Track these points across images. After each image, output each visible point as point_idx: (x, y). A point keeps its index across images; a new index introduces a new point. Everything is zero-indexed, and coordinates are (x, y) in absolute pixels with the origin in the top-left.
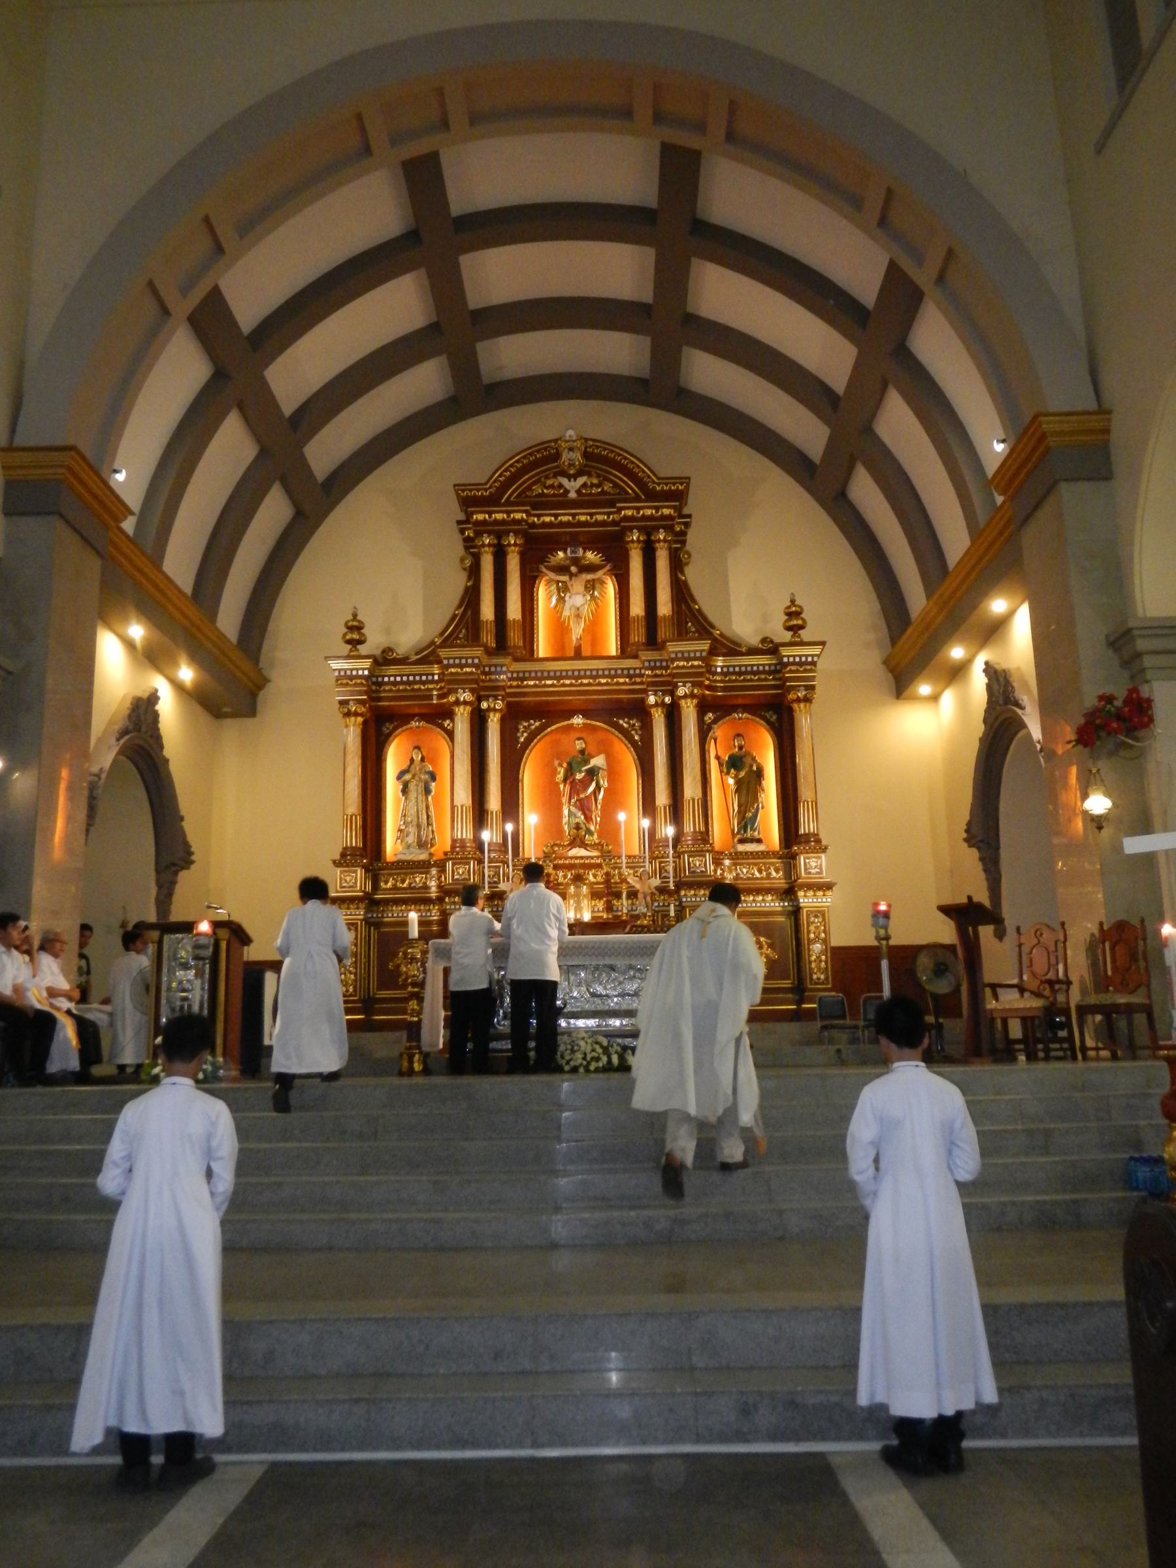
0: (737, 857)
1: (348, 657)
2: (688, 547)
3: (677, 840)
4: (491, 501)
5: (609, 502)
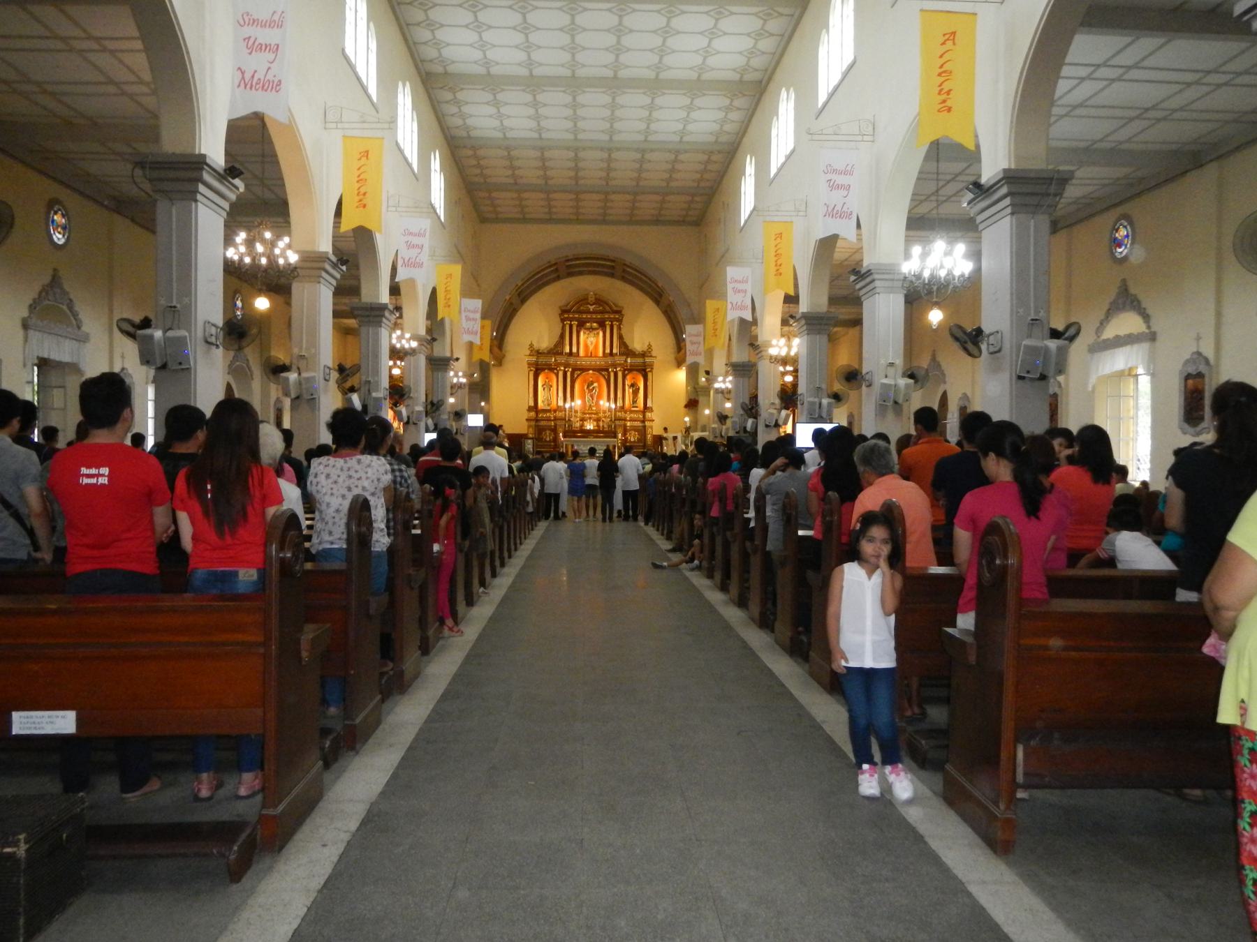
0: (632, 412)
3: (615, 409)
5: (601, 312)
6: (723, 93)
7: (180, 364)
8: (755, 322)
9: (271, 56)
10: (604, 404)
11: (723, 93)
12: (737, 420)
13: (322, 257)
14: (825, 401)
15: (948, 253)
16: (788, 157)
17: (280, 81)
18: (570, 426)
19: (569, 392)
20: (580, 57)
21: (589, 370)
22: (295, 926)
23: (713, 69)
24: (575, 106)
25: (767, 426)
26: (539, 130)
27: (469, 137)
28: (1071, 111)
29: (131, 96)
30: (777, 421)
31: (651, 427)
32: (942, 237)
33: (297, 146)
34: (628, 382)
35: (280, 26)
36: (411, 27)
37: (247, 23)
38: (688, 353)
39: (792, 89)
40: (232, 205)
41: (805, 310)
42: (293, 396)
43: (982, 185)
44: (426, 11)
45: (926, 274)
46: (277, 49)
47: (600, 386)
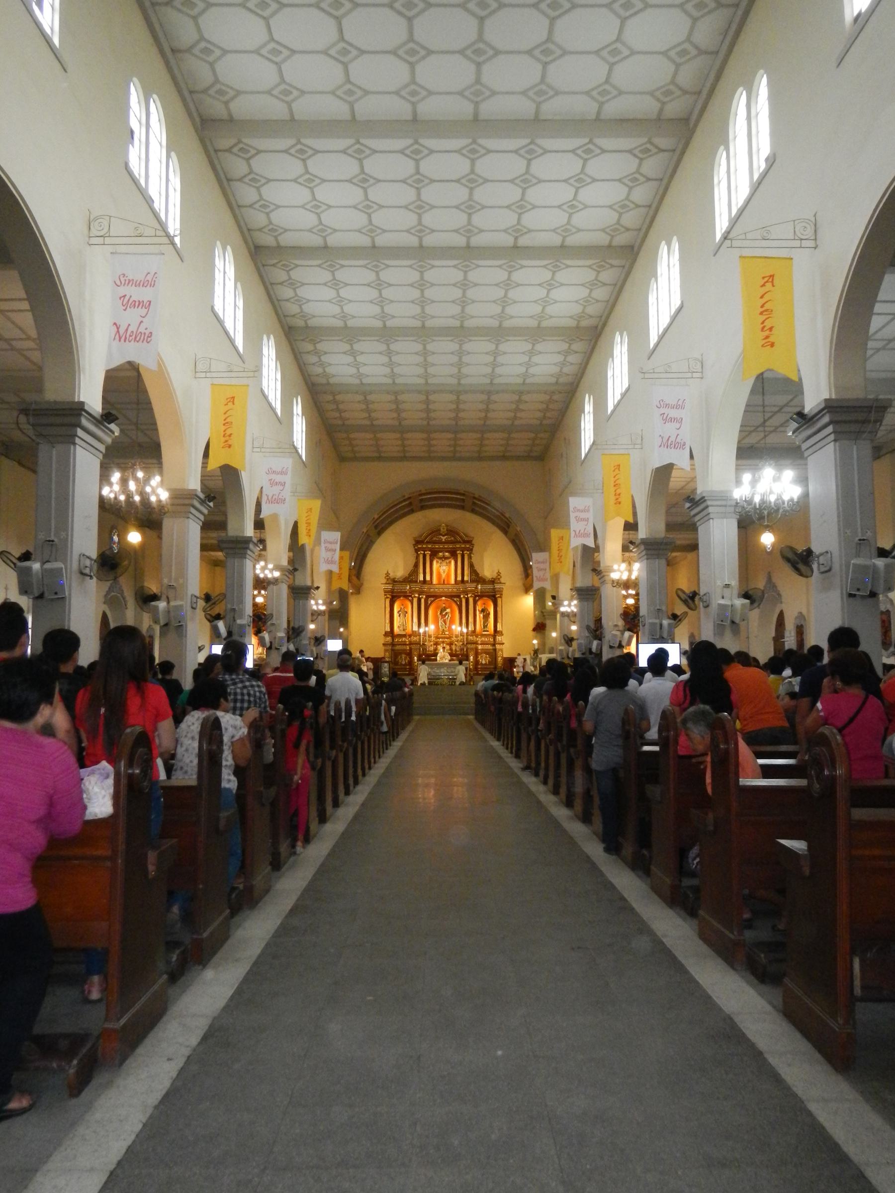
0: (483, 635)
1: (386, 584)
2: (474, 552)
3: (467, 633)
4: (422, 542)
6: (562, 338)
7: (56, 593)
8: (597, 549)
9: (144, 311)
10: (456, 628)
11: (562, 338)
12: (583, 642)
13: (192, 495)
14: (665, 622)
15: (776, 479)
16: (623, 395)
17: (151, 333)
18: (425, 649)
19: (422, 617)
20: (429, 310)
21: (442, 596)
22: (129, 1142)
23: (551, 317)
24: (425, 353)
25: (611, 647)
26: (393, 375)
27: (328, 384)
28: (887, 344)
29: (19, 351)
30: (620, 642)
31: (502, 650)
32: (770, 465)
33: (169, 394)
34: (479, 608)
35: (152, 284)
36: (274, 287)
37: (123, 282)
38: (535, 579)
39: (625, 333)
40: (108, 448)
41: (644, 537)
42: (162, 623)
43: (806, 415)
44: (288, 271)
45: (757, 499)
46: (150, 304)
47: (452, 612)
